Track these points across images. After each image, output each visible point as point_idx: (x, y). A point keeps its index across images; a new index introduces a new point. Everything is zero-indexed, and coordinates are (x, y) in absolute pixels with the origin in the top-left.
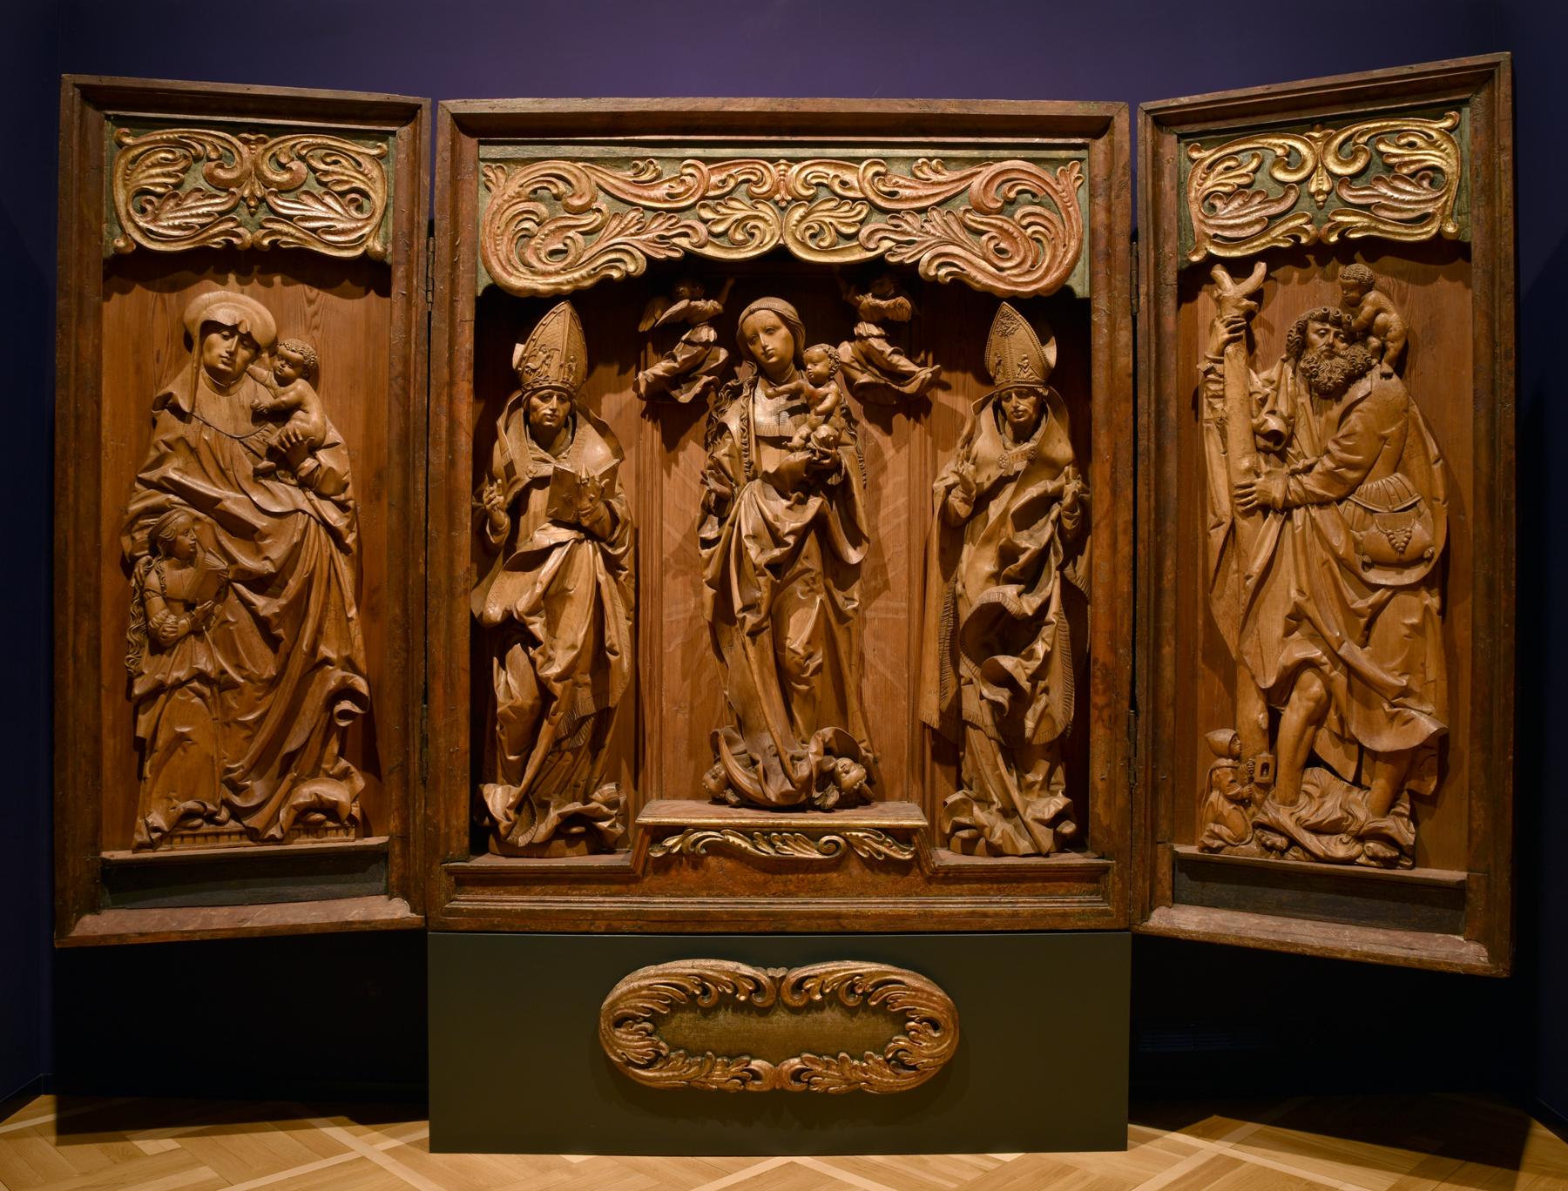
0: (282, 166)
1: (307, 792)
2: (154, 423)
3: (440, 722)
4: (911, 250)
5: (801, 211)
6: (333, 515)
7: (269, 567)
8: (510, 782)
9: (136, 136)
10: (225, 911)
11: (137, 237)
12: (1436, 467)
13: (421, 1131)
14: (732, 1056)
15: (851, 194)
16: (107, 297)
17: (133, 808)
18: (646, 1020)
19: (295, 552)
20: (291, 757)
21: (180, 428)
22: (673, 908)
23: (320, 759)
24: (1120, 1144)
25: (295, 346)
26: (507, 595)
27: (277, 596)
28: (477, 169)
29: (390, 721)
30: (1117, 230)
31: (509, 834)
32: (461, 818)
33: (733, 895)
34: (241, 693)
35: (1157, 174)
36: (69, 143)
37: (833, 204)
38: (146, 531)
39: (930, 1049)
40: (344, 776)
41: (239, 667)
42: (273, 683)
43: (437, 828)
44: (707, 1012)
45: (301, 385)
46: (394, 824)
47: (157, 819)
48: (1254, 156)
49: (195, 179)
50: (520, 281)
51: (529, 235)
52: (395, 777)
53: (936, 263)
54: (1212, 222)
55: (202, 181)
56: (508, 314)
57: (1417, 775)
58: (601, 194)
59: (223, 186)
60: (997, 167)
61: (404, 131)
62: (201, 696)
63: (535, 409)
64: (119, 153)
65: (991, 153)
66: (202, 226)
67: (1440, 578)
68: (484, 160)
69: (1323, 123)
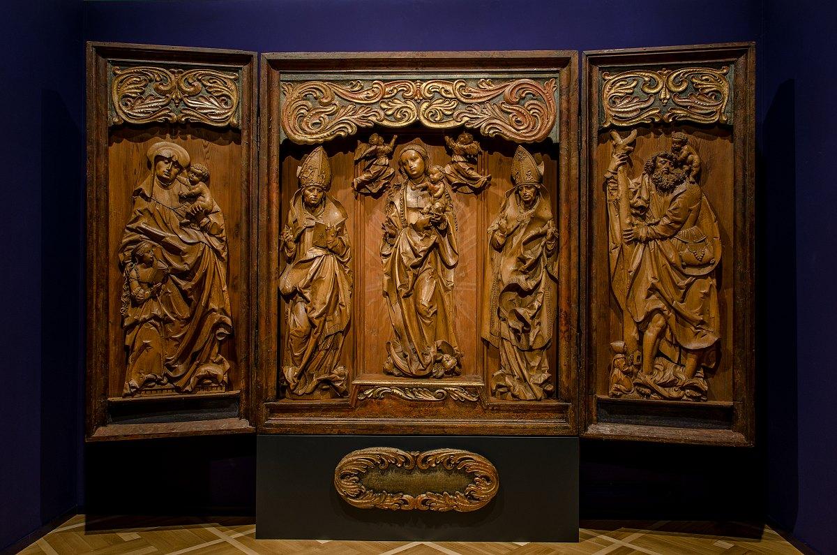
0: (190, 84)
1: (203, 370)
2: (134, 202)
3: (263, 338)
4: (477, 122)
5: (426, 105)
6: (216, 244)
7: (187, 268)
8: (296, 365)
9: (122, 70)
10: (165, 425)
11: (124, 117)
12: (715, 224)
13: (253, 530)
14: (395, 493)
15: (450, 96)
16: (110, 144)
17: (123, 378)
18: (355, 475)
19: (198, 261)
20: (196, 354)
21: (146, 205)
22: (368, 423)
23: (209, 355)
24: (575, 539)
25: (199, 167)
26: (290, 279)
27: (190, 280)
28: (279, 85)
29: (242, 337)
30: (572, 111)
31: (295, 389)
32: (272, 383)
33: (396, 417)
34: (174, 325)
35: (590, 85)
36: (91, 73)
37: (441, 101)
38: (130, 251)
39: (486, 491)
40: (221, 362)
41: (173, 313)
42: (188, 321)
43: (262, 387)
44: (383, 472)
45: (201, 185)
46: (242, 384)
47: (134, 383)
48: (634, 80)
49: (150, 90)
50: (300, 137)
51: (303, 116)
52: (243, 363)
53: (488, 127)
54: (613, 109)
55: (153, 91)
56: (294, 151)
57: (708, 361)
58: (336, 97)
59: (163, 93)
60: (517, 82)
61: (245, 68)
62: (155, 326)
63: (307, 195)
64: (114, 78)
65: (514, 76)
66: (153, 112)
67: (718, 273)
68: (282, 81)
69: (667, 67)
